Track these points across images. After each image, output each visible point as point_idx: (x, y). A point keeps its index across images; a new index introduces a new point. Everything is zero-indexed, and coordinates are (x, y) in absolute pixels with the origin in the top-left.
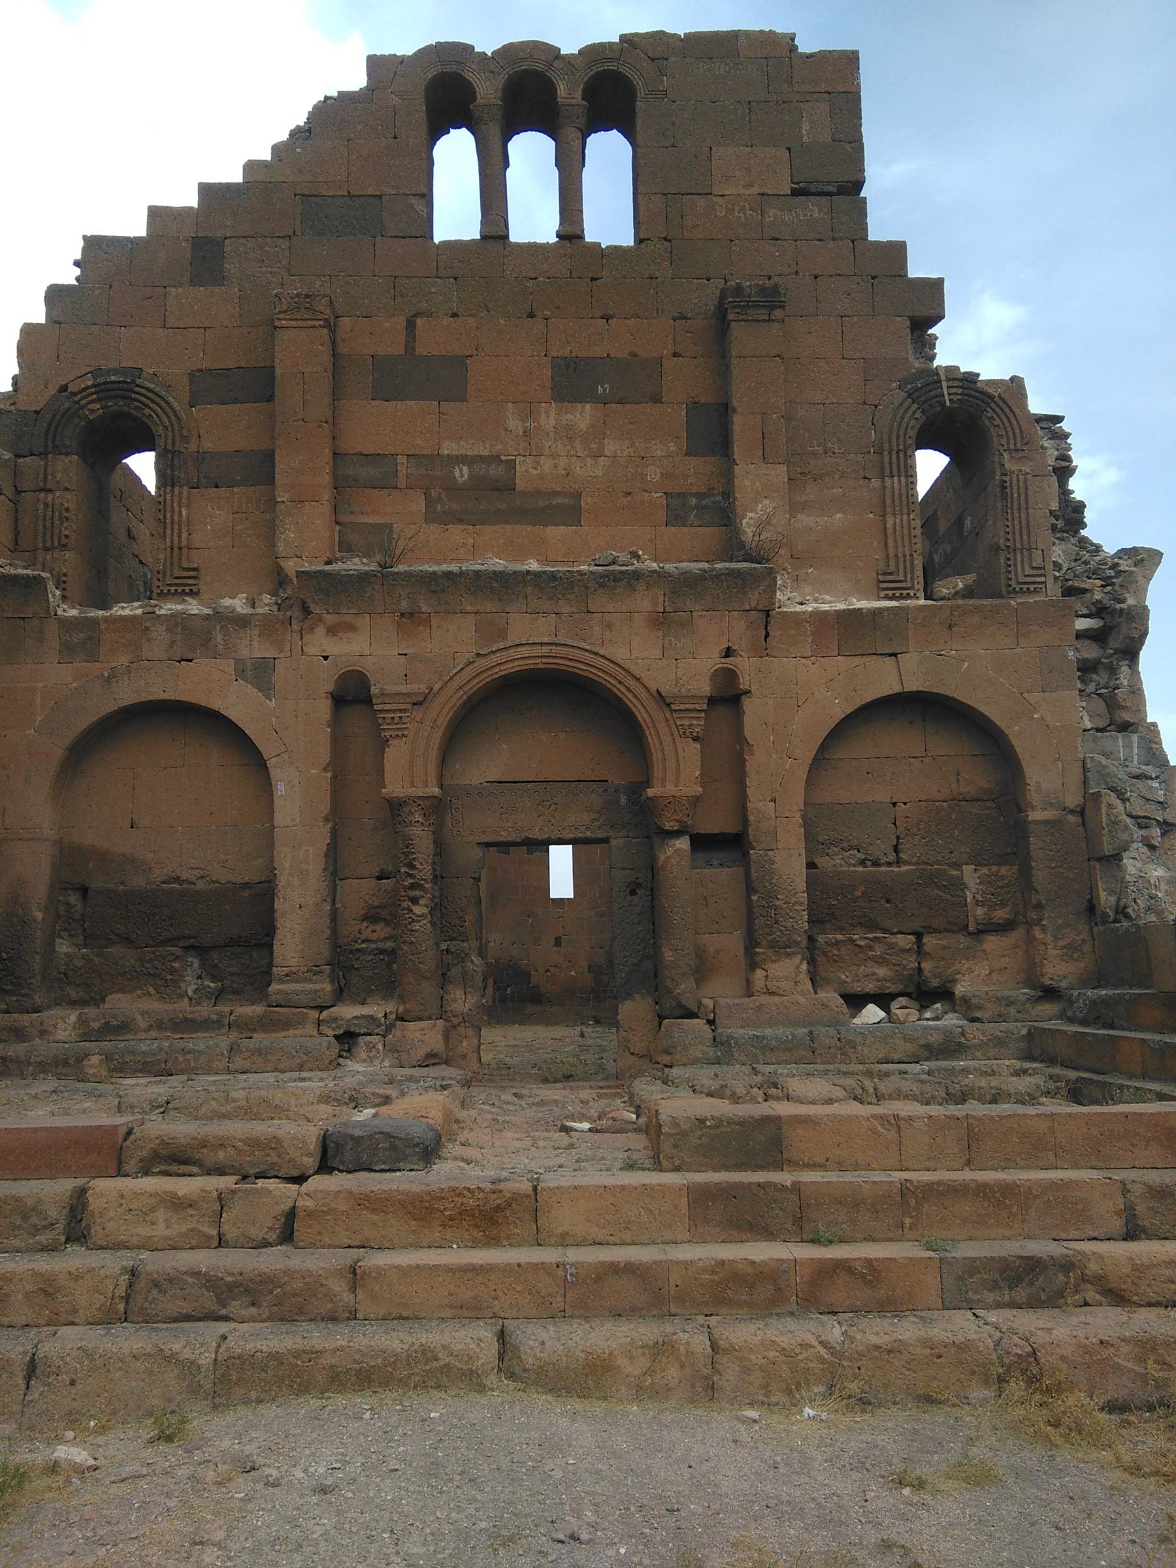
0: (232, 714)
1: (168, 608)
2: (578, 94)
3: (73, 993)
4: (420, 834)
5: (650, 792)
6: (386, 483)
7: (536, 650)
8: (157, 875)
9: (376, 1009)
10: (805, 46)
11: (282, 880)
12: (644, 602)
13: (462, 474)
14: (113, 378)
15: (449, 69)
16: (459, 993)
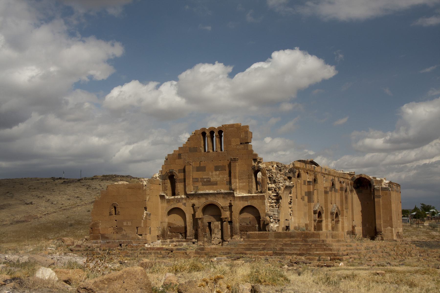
0: (182, 209)
1: (176, 197)
2: (217, 133)
3: (170, 238)
4: (199, 222)
5: (221, 217)
6: (198, 181)
7: (210, 202)
8: (177, 226)
9: (196, 240)
10: (242, 125)
11: (187, 226)
12: (221, 196)
13: (205, 180)
14: (171, 171)
15: (203, 131)
16: (206, 239)
